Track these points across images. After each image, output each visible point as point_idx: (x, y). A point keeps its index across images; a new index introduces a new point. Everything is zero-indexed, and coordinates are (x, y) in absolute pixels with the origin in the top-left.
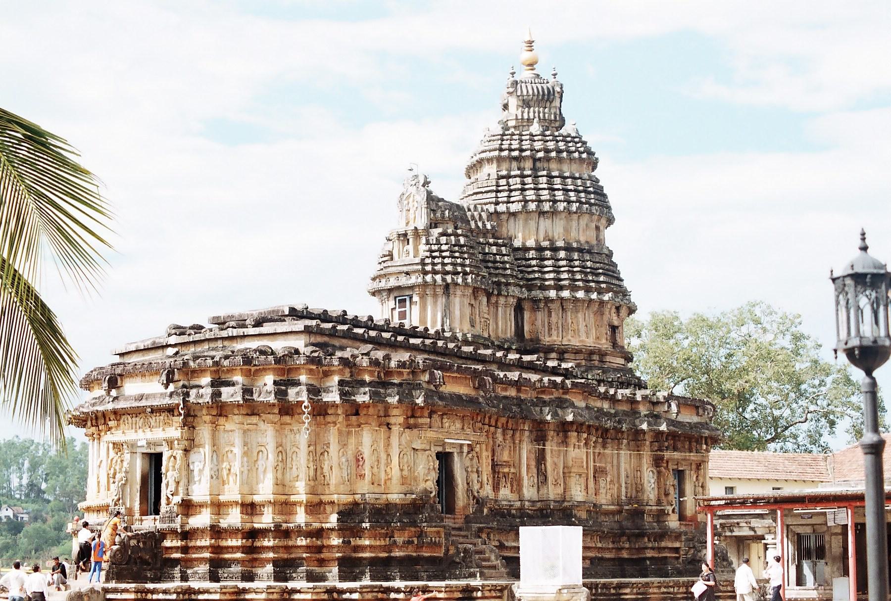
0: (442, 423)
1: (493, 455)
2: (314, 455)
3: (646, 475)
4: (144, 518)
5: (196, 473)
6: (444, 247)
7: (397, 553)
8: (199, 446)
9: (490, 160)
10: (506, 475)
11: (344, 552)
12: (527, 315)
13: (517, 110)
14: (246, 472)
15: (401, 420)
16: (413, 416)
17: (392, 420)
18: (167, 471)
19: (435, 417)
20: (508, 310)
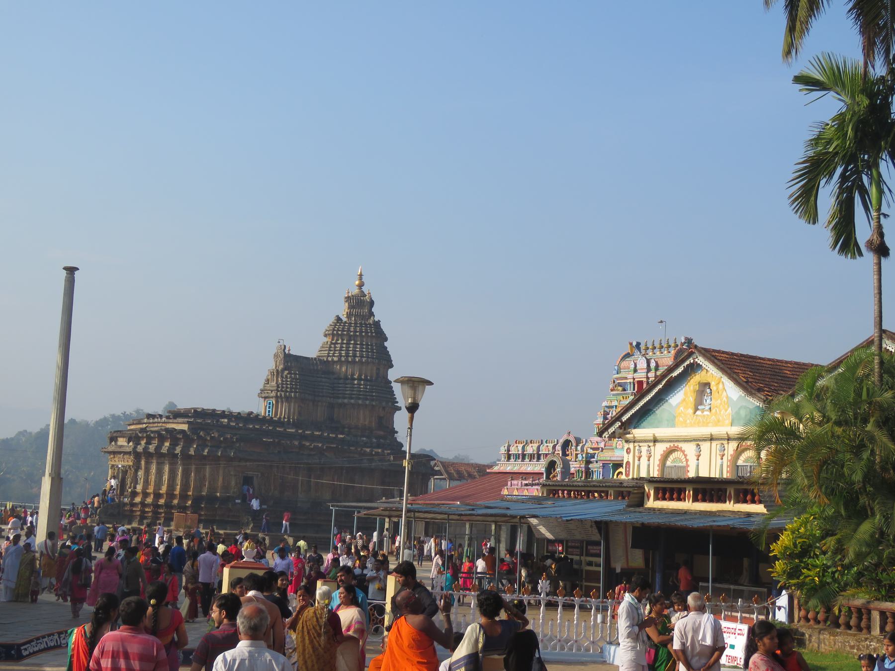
5: (139, 479)
6: (289, 380)
7: (217, 518)
18: (128, 478)
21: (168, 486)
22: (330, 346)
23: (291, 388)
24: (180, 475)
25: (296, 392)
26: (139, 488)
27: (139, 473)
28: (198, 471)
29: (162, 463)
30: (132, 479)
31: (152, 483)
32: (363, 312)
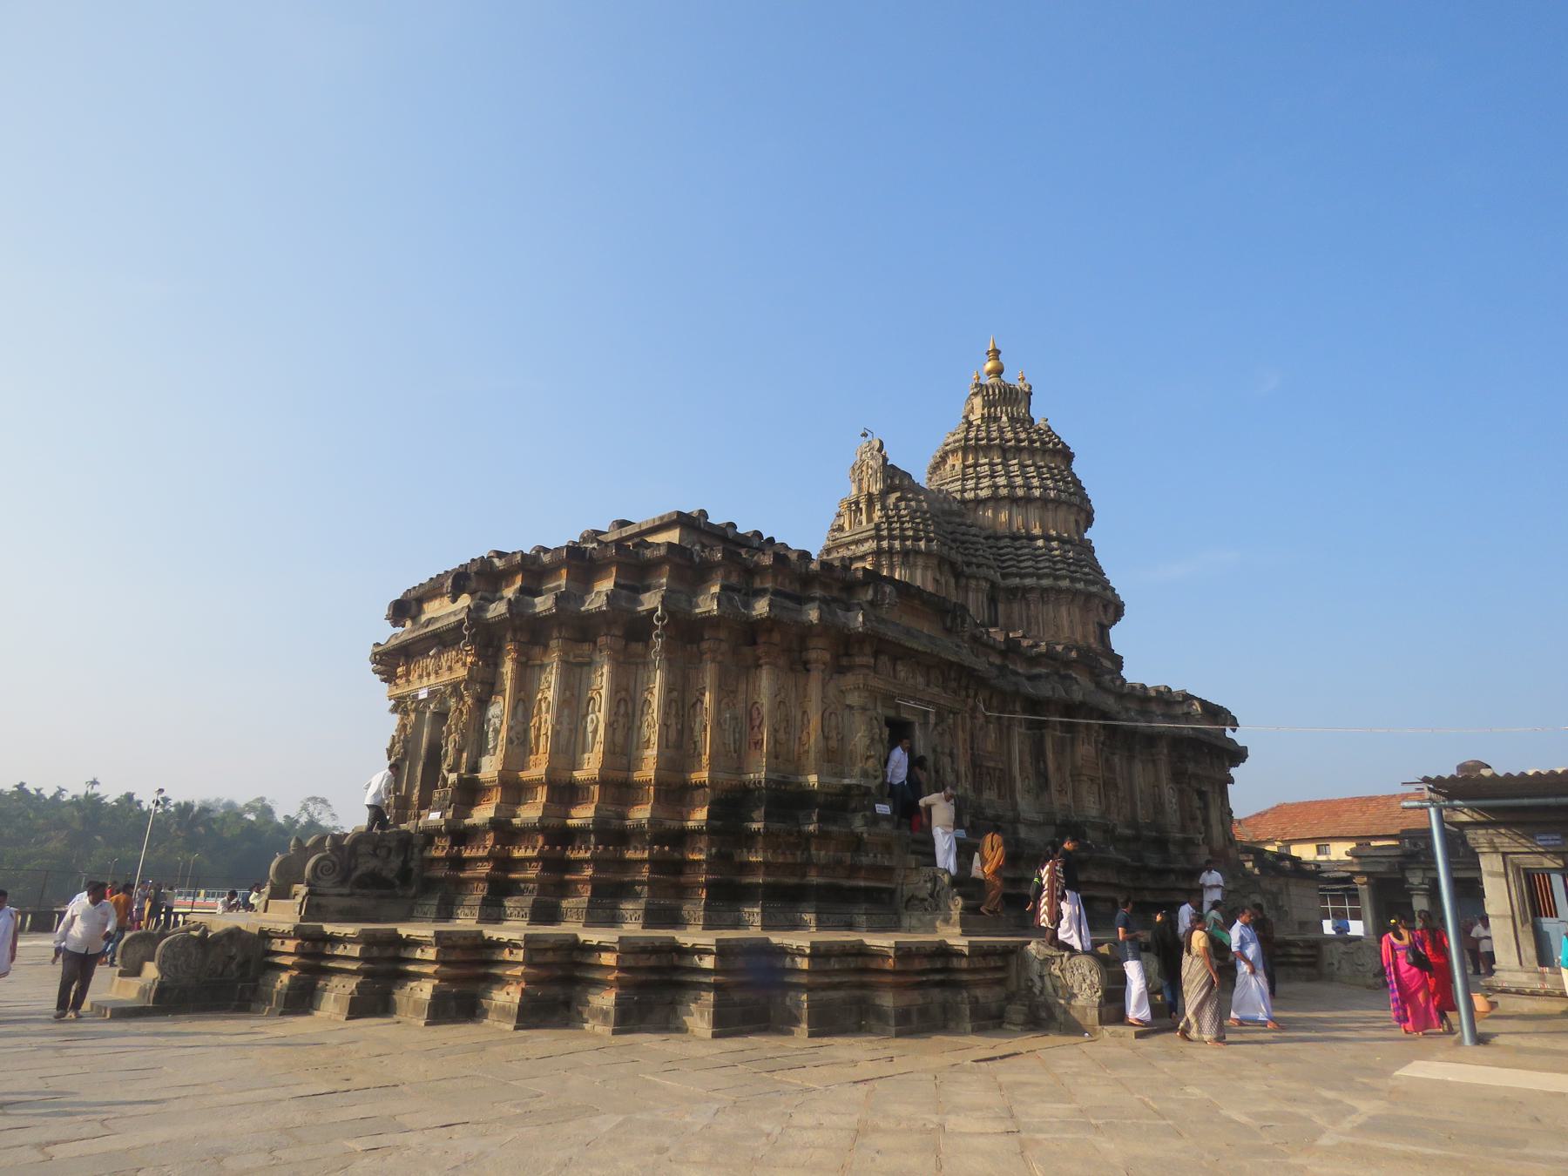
0: (894, 669)
1: (972, 742)
2: (680, 705)
3: (1166, 791)
4: (422, 812)
5: (491, 735)
6: (903, 512)
7: (814, 878)
8: (498, 694)
9: (954, 451)
10: (991, 771)
11: (721, 875)
12: (1001, 607)
13: (983, 409)
14: (565, 734)
15: (827, 656)
16: (847, 654)
17: (813, 655)
18: (449, 733)
19: (884, 659)
20: (980, 595)
21: (611, 751)
22: (964, 474)
23: (916, 530)
24: (655, 705)
25: (929, 540)
26: (490, 768)
27: (494, 711)
28: (725, 692)
29: (581, 665)
30: (463, 736)
31: (544, 745)
32: (1018, 414)
